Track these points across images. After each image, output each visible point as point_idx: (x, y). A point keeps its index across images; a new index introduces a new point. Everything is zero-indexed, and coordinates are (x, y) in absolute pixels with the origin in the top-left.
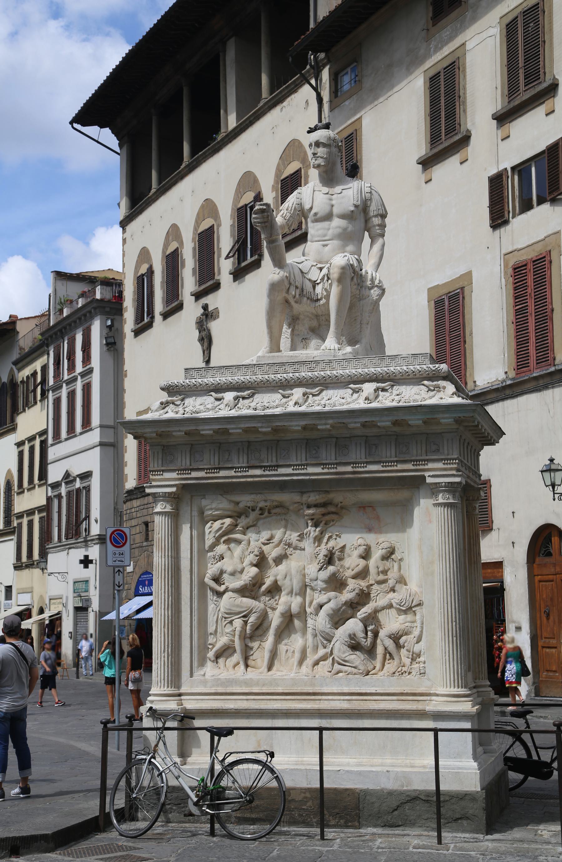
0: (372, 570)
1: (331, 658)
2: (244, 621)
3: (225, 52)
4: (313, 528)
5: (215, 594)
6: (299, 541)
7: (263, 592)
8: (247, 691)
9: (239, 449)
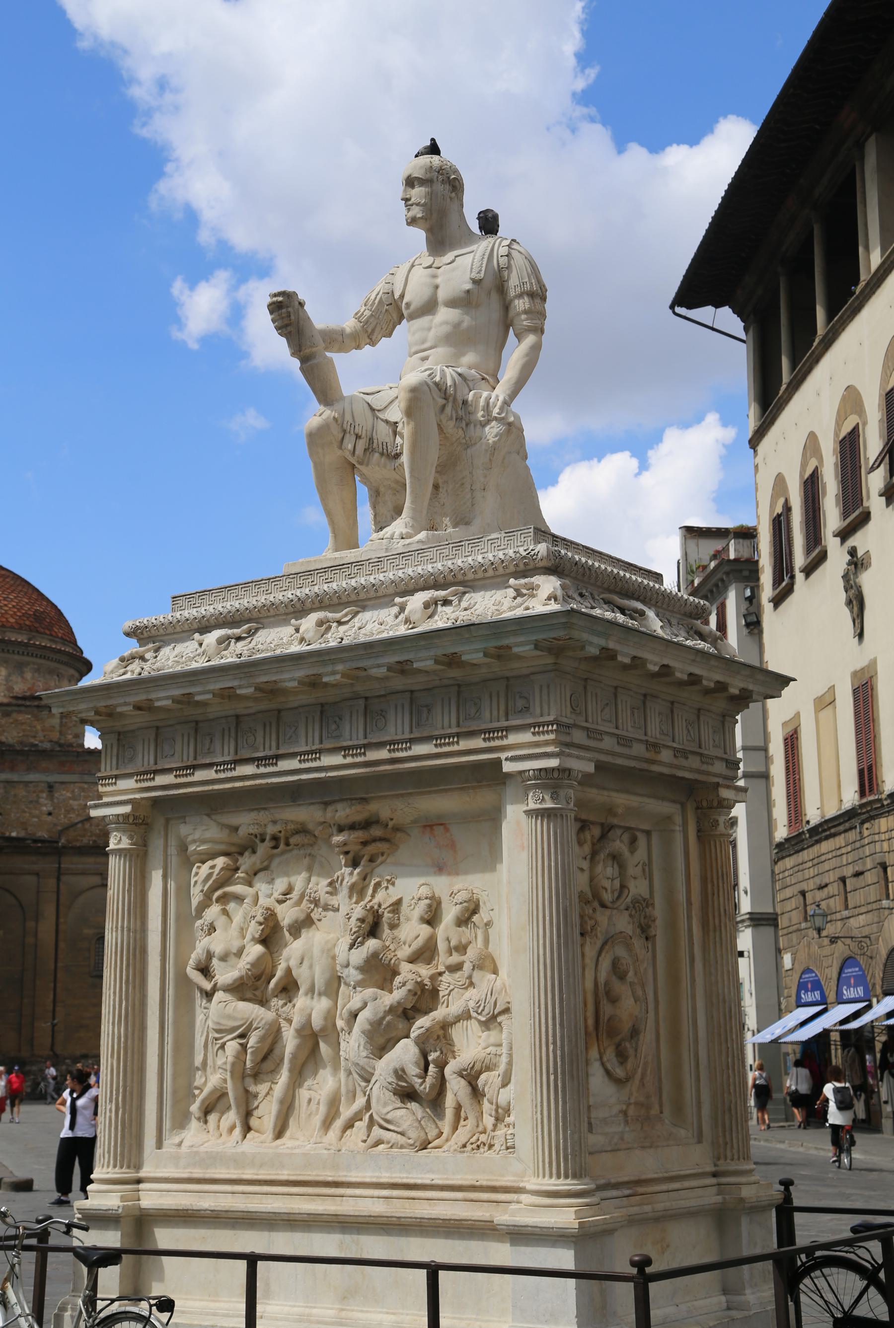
0: (442, 946)
1: (368, 1115)
2: (241, 1044)
3: (862, 159)
4: (349, 870)
5: (204, 995)
6: (331, 893)
7: (274, 990)
8: (234, 1177)
9: (223, 729)
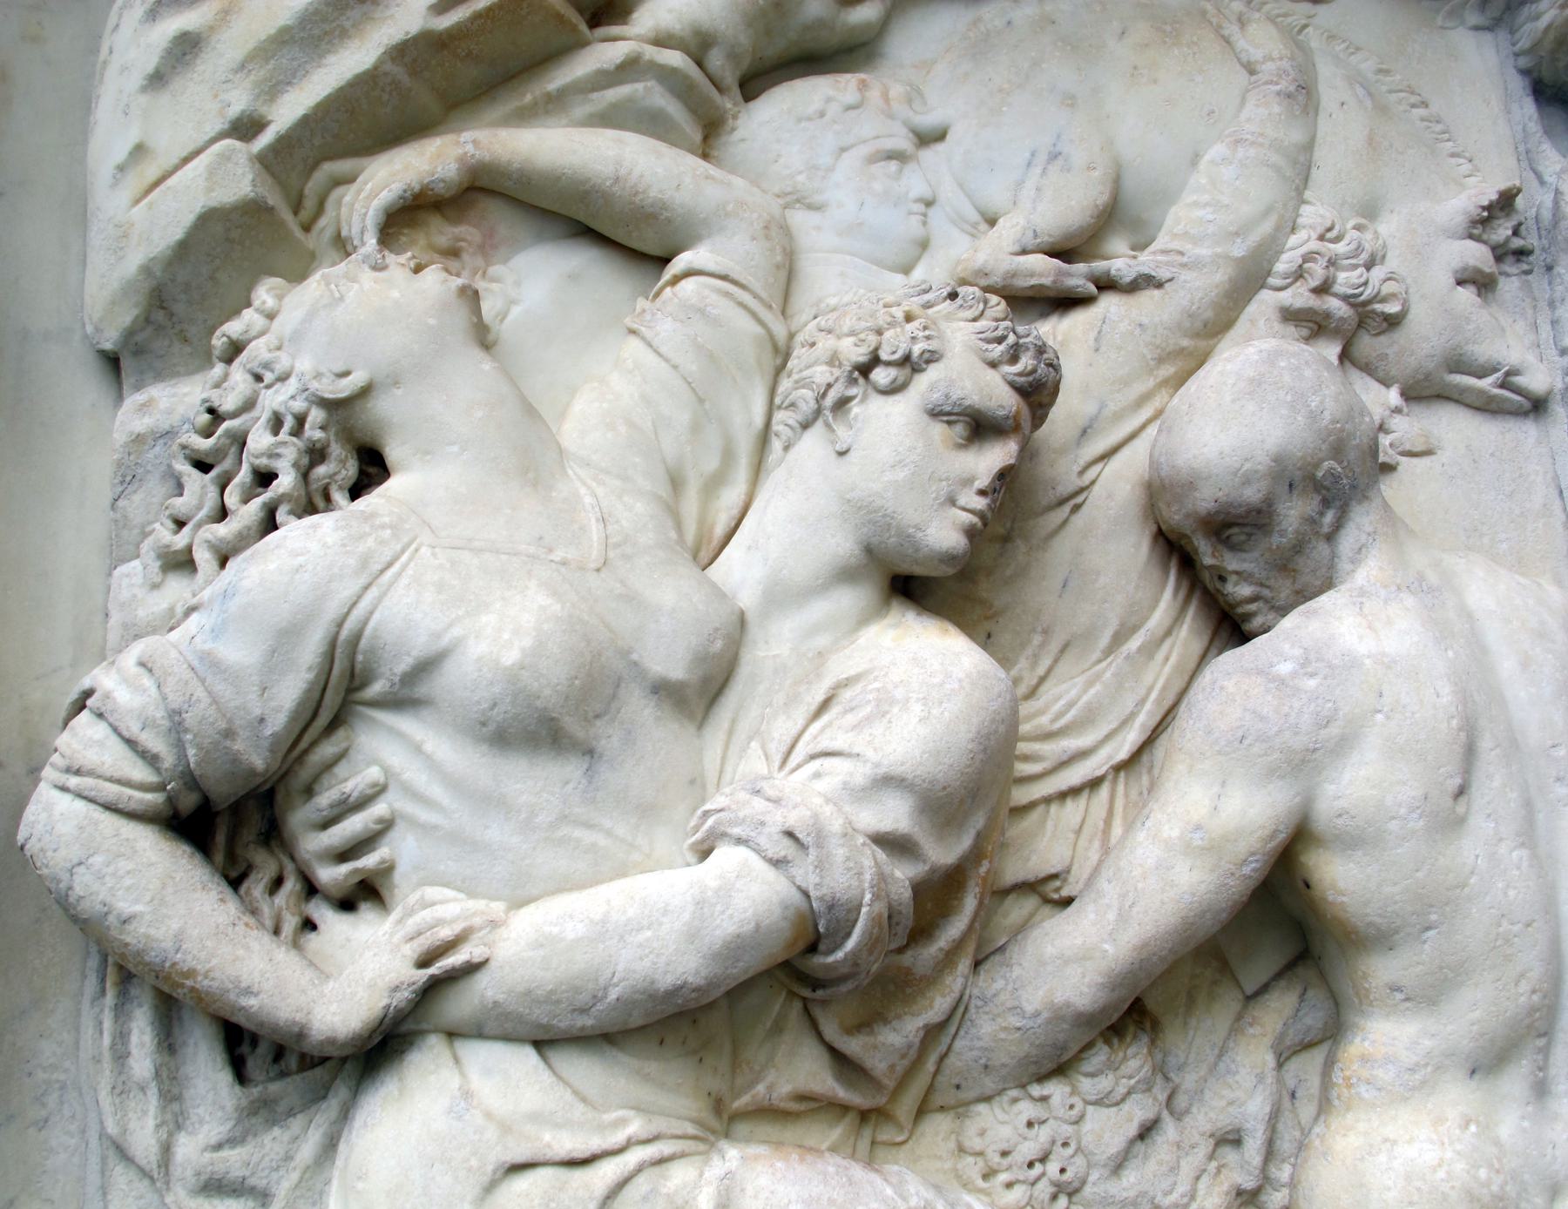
6: (1481, 283)
